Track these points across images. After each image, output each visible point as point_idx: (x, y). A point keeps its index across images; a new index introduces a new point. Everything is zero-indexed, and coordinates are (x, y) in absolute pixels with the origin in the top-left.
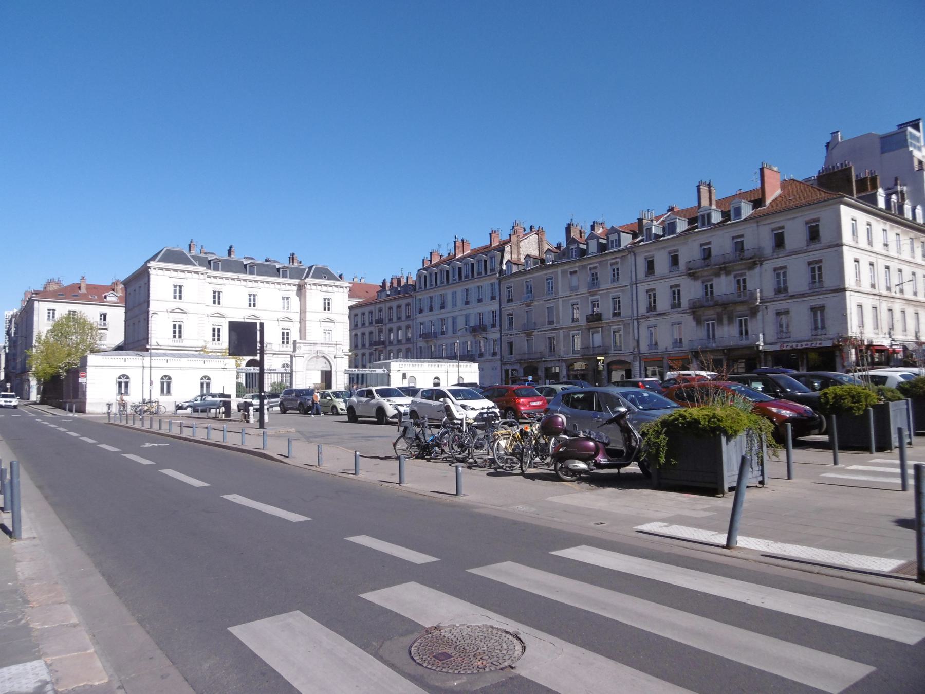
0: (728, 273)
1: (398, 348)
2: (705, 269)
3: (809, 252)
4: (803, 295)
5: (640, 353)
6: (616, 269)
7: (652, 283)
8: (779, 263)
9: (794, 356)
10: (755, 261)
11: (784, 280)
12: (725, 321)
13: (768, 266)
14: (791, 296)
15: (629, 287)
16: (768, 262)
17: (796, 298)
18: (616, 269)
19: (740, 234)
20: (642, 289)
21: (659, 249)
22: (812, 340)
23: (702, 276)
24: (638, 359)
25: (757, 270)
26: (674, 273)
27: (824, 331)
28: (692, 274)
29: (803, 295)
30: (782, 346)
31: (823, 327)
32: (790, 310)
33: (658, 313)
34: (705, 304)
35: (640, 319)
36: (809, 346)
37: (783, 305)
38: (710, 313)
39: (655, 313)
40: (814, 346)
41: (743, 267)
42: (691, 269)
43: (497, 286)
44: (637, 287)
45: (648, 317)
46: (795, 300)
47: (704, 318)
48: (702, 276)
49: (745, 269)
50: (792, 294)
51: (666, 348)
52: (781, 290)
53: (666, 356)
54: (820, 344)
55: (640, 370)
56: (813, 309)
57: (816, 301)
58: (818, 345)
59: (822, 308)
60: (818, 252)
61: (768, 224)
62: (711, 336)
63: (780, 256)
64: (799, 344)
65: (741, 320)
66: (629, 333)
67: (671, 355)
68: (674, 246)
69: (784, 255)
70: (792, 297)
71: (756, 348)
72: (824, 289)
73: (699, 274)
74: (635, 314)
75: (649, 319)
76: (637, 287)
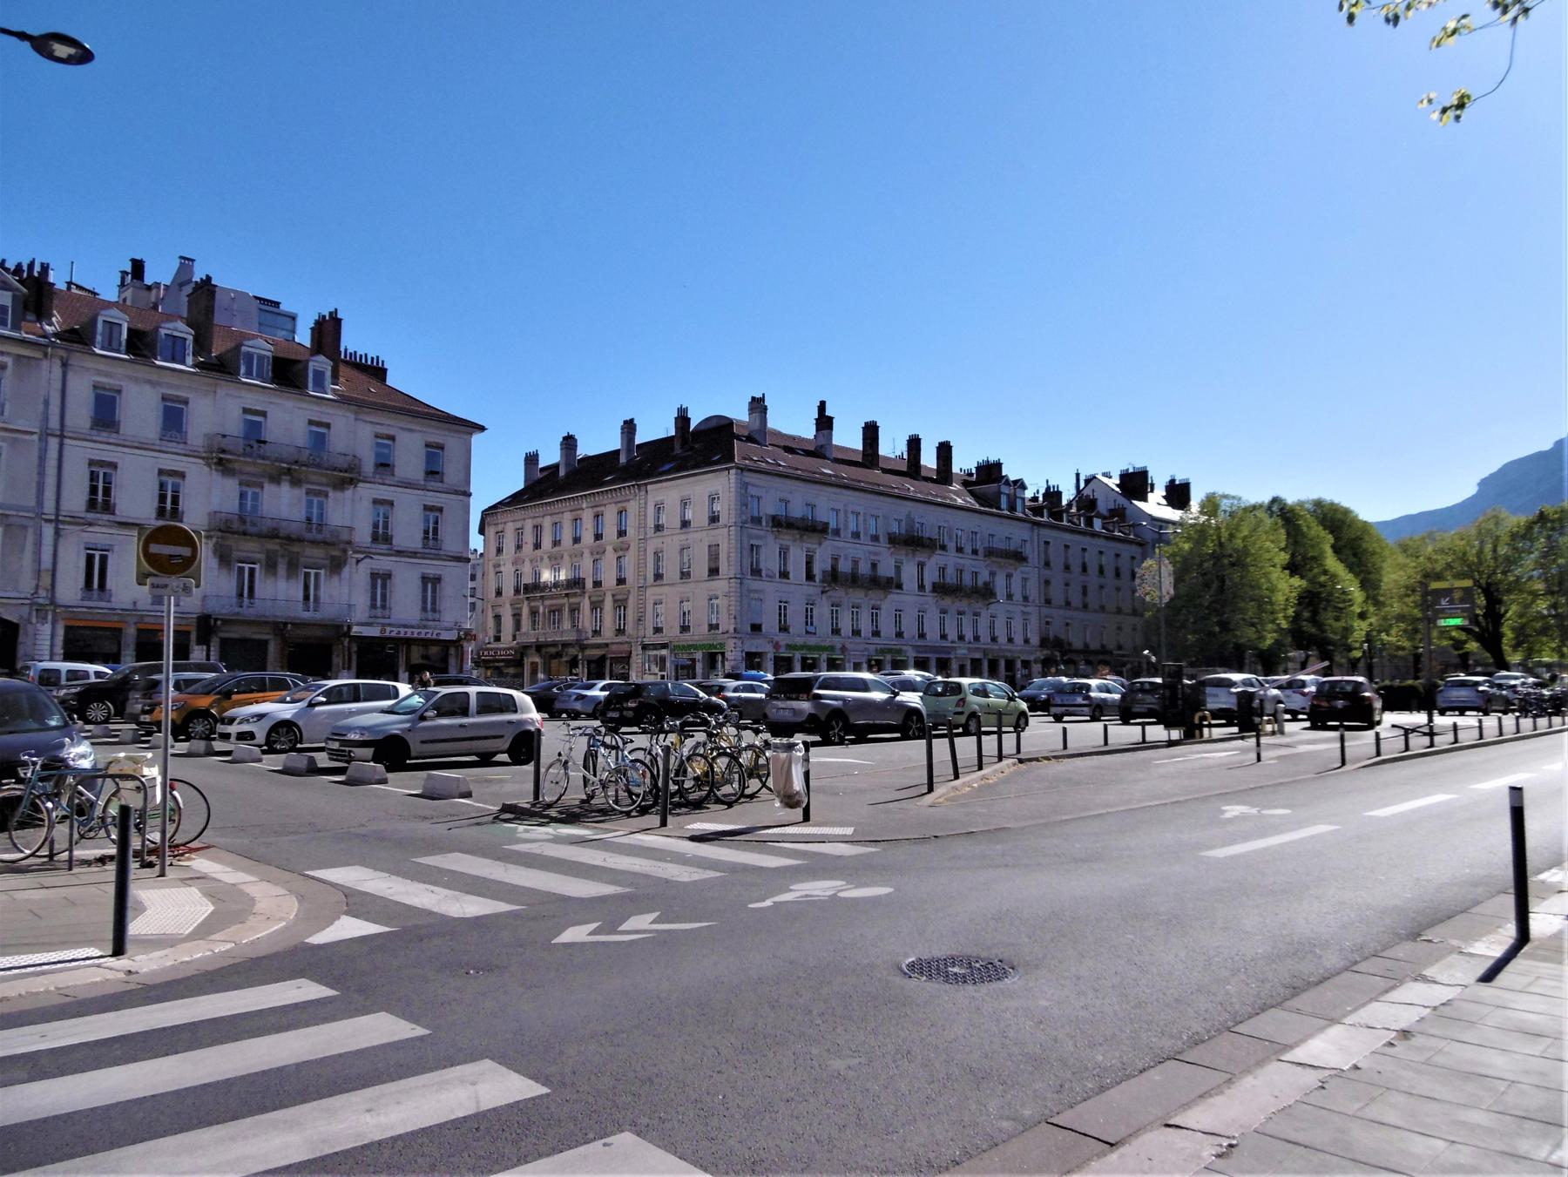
0: (296, 482)
1: (214, 562)
2: (242, 459)
3: (428, 490)
4: (414, 554)
5: (53, 601)
6: (1002, 663)
7: (108, 447)
8: (384, 492)
9: (390, 649)
10: (347, 477)
11: (312, 508)
12: (282, 569)
13: (366, 493)
14: (398, 551)
15: (35, 437)
16: (368, 485)
17: (404, 556)
18: (1002, 663)
19: (324, 420)
20: (78, 458)
21: (137, 380)
22: (425, 627)
23: (241, 473)
24: (50, 617)
25: (349, 493)
26: (174, 444)
27: (437, 616)
28: (221, 460)
29: (414, 554)
30: (383, 631)
31: (384, 607)
32: (394, 573)
33: (118, 519)
34: (308, 536)
35: (64, 522)
36: (423, 636)
37: (384, 563)
38: (250, 547)
39: (111, 518)
40: (429, 636)
41: (324, 480)
42: (223, 451)
43: (311, 487)
44: (61, 445)
45: (90, 524)
46: (403, 559)
47: (235, 554)
48: (241, 473)
49: (328, 485)
50: (399, 549)
51: (135, 603)
52: (382, 536)
53: (132, 620)
54: (438, 634)
55: (52, 645)
56: (425, 579)
57: (432, 567)
58: (434, 636)
59: (387, 576)
60: (438, 494)
61: (372, 423)
62: (246, 590)
63: (387, 482)
64: (402, 630)
65: (309, 573)
66: (22, 550)
67: (147, 620)
68: (178, 387)
69: (392, 483)
70: (400, 553)
71: (345, 629)
72: (442, 552)
73: (236, 466)
74: (49, 506)
75: (90, 529)
76: (61, 445)
